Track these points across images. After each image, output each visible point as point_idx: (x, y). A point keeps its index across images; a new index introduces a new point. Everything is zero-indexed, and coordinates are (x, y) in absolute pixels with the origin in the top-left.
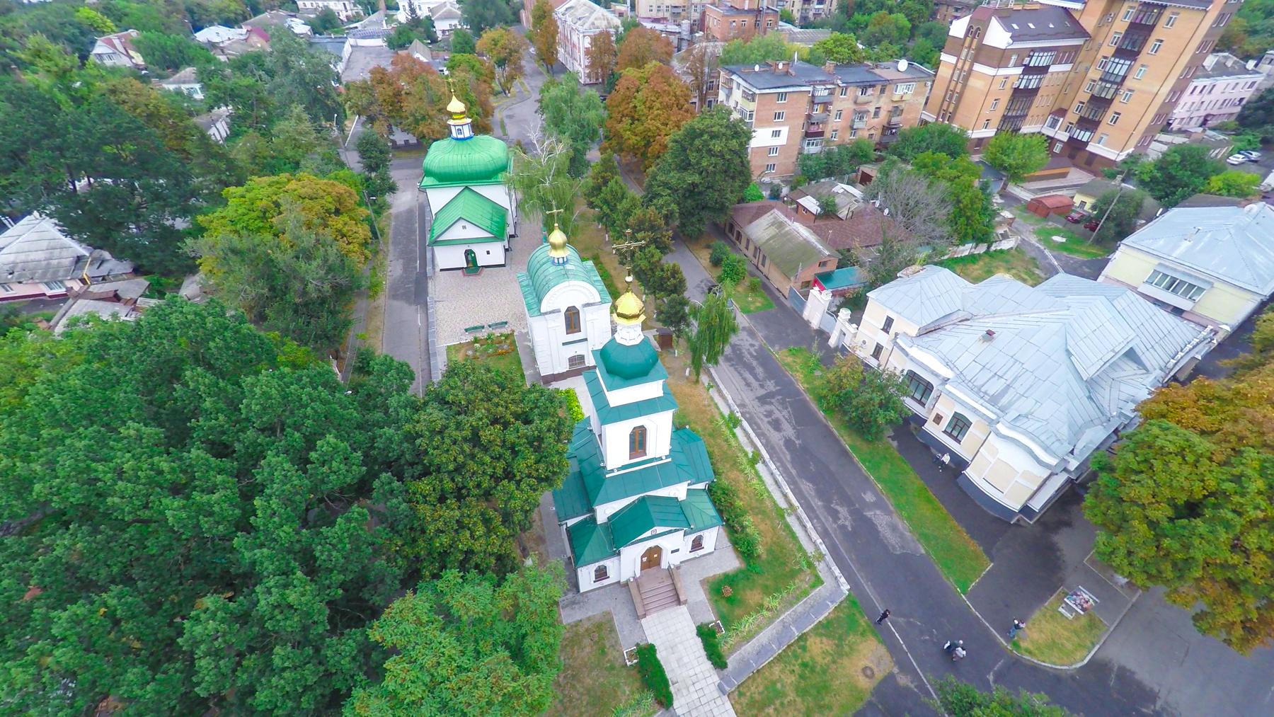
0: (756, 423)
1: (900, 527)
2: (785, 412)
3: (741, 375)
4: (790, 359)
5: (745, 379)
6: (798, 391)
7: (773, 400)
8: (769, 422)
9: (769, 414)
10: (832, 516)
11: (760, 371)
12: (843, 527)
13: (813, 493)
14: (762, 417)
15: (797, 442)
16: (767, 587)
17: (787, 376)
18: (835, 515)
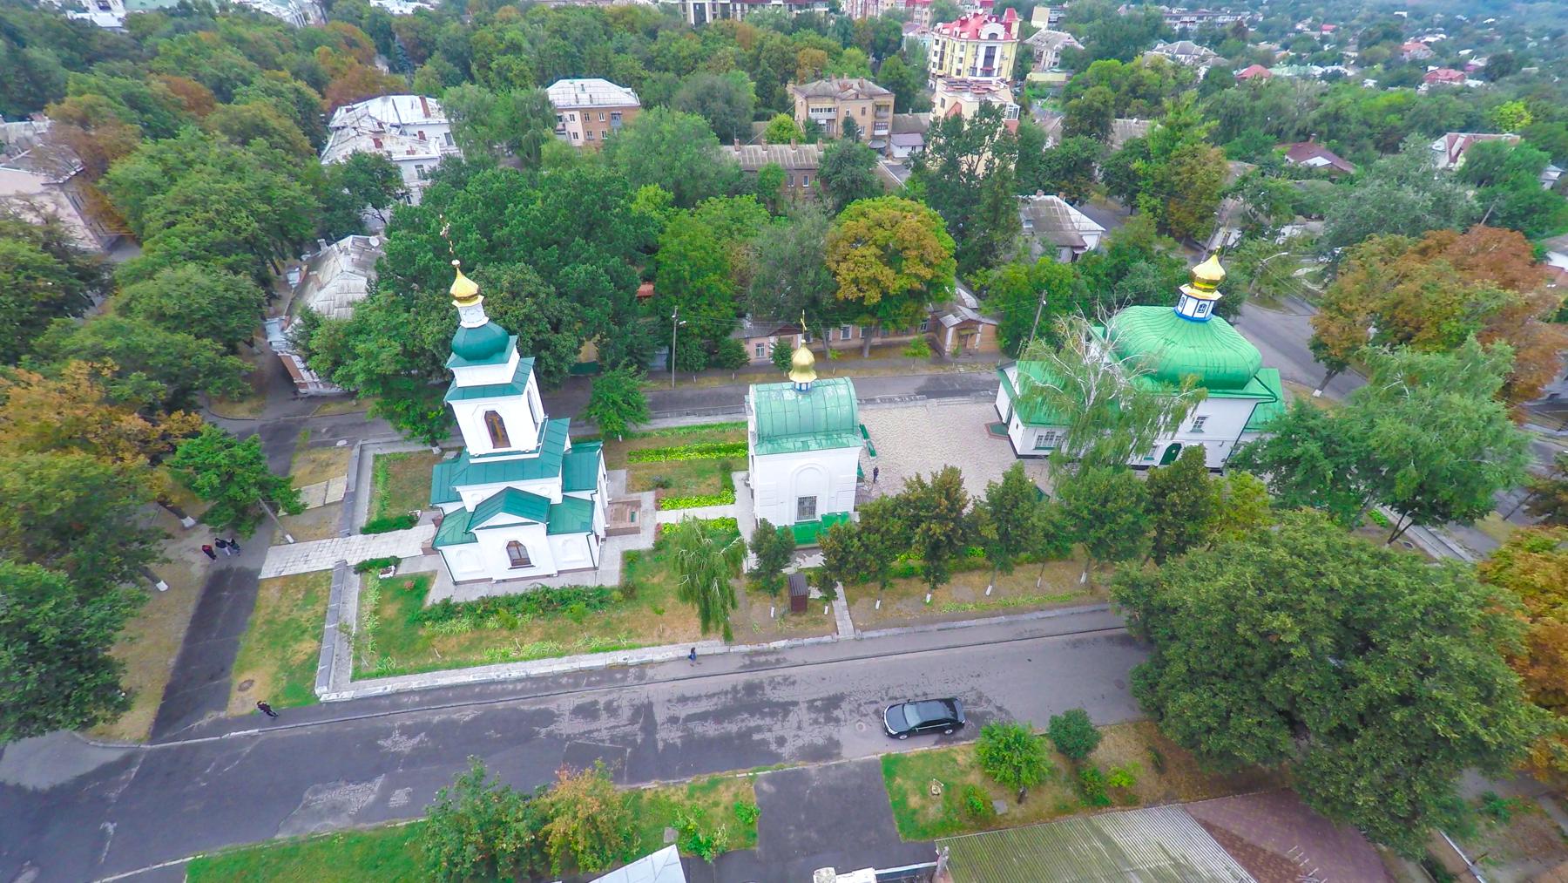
0: (599, 683)
1: (330, 822)
2: (605, 734)
3: (709, 696)
4: (725, 797)
5: (698, 698)
6: (647, 780)
7: (637, 727)
8: (596, 702)
9: (611, 710)
10: (409, 726)
11: (711, 729)
12: (388, 735)
13: (455, 716)
14: (615, 695)
15: (544, 731)
16: (391, 624)
17: (686, 772)
18: (410, 732)
